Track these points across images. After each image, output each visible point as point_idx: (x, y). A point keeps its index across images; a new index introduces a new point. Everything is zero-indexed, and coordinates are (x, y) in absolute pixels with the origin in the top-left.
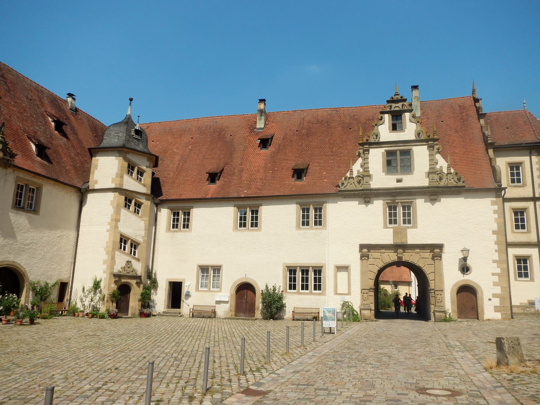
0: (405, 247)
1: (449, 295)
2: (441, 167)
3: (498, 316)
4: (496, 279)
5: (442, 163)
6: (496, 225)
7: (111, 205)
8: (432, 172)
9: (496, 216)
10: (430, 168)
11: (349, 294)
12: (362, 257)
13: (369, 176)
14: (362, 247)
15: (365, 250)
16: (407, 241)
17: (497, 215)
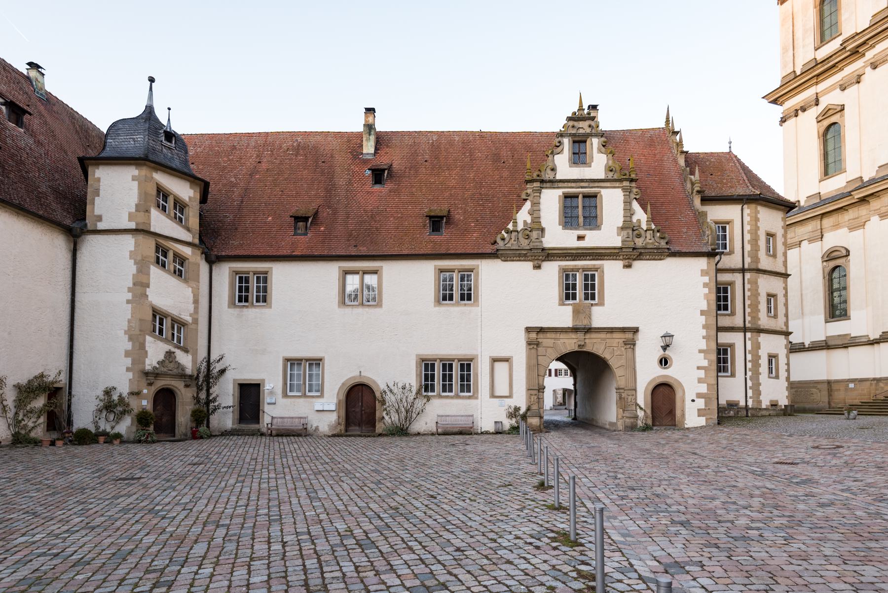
0: (588, 330)
1: (643, 396)
2: (639, 221)
3: (702, 421)
4: (702, 374)
5: (640, 216)
6: (705, 302)
7: (130, 258)
8: (629, 227)
9: (706, 290)
10: (624, 221)
11: (510, 396)
12: (529, 343)
13: (543, 230)
14: (528, 330)
15: (533, 335)
16: (590, 323)
17: (707, 289)
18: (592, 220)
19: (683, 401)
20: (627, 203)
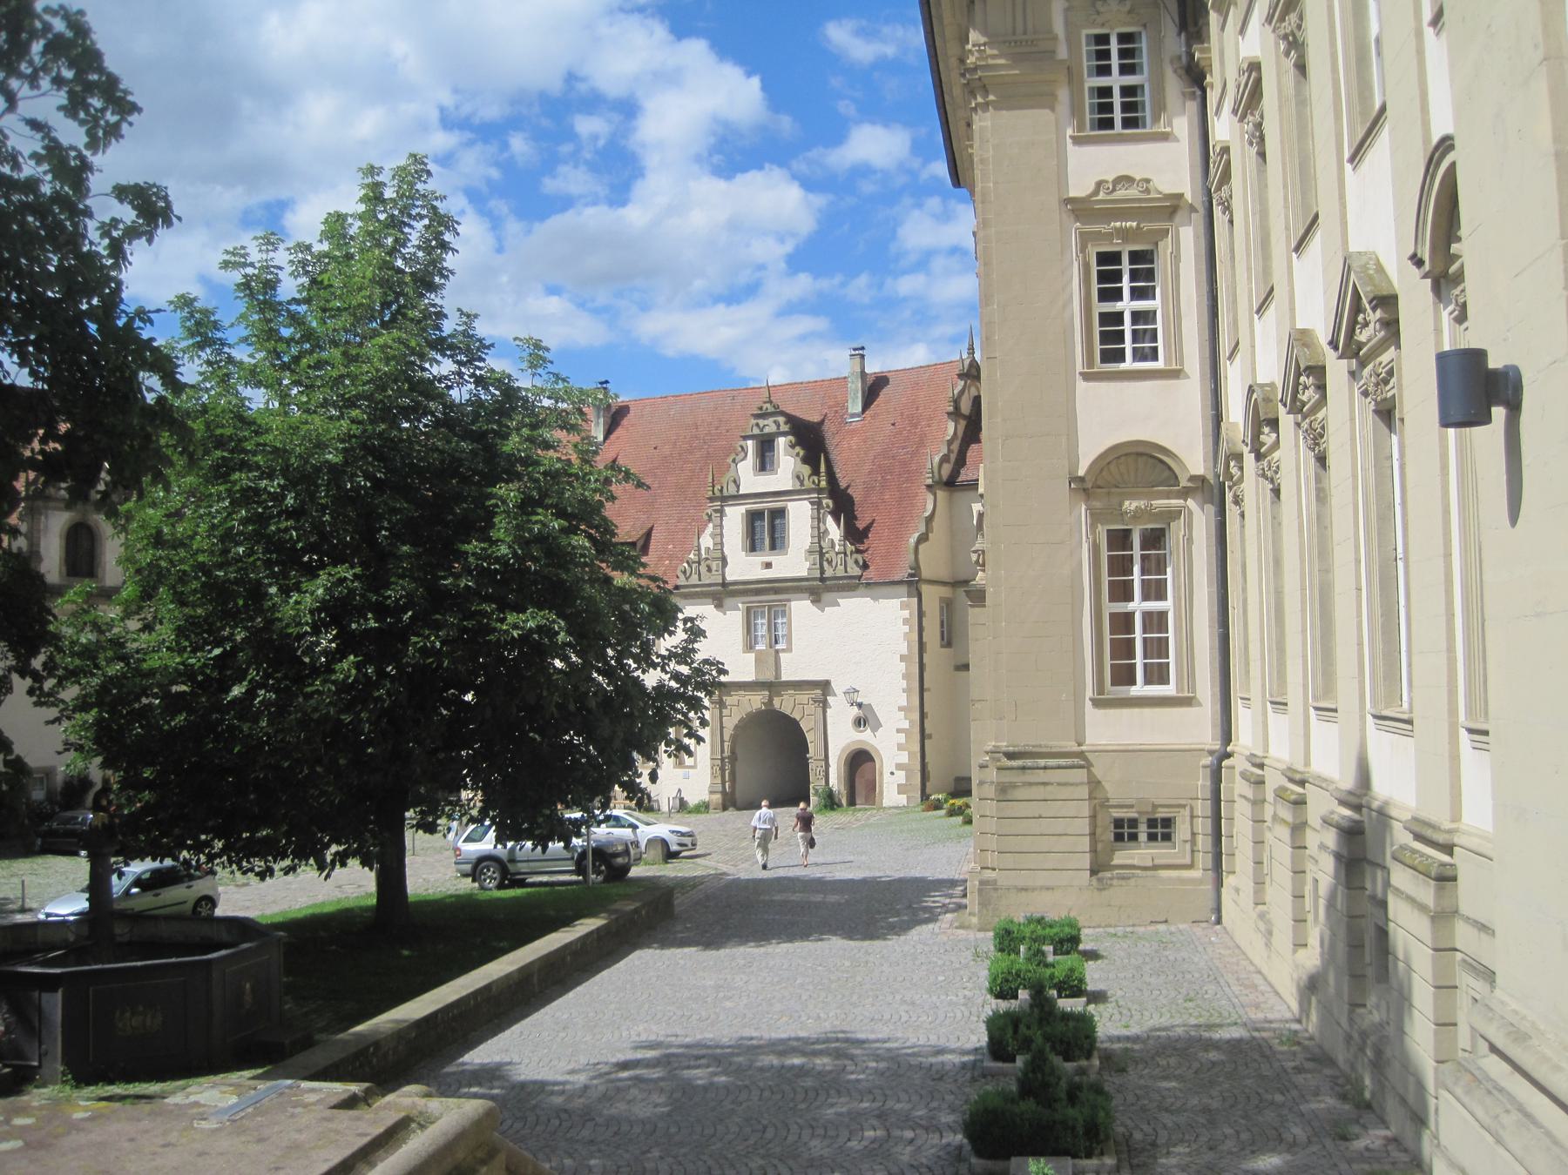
3: (902, 800)
4: (902, 738)
8: (819, 552)
18: (777, 542)
19: (881, 774)
20: (819, 519)
